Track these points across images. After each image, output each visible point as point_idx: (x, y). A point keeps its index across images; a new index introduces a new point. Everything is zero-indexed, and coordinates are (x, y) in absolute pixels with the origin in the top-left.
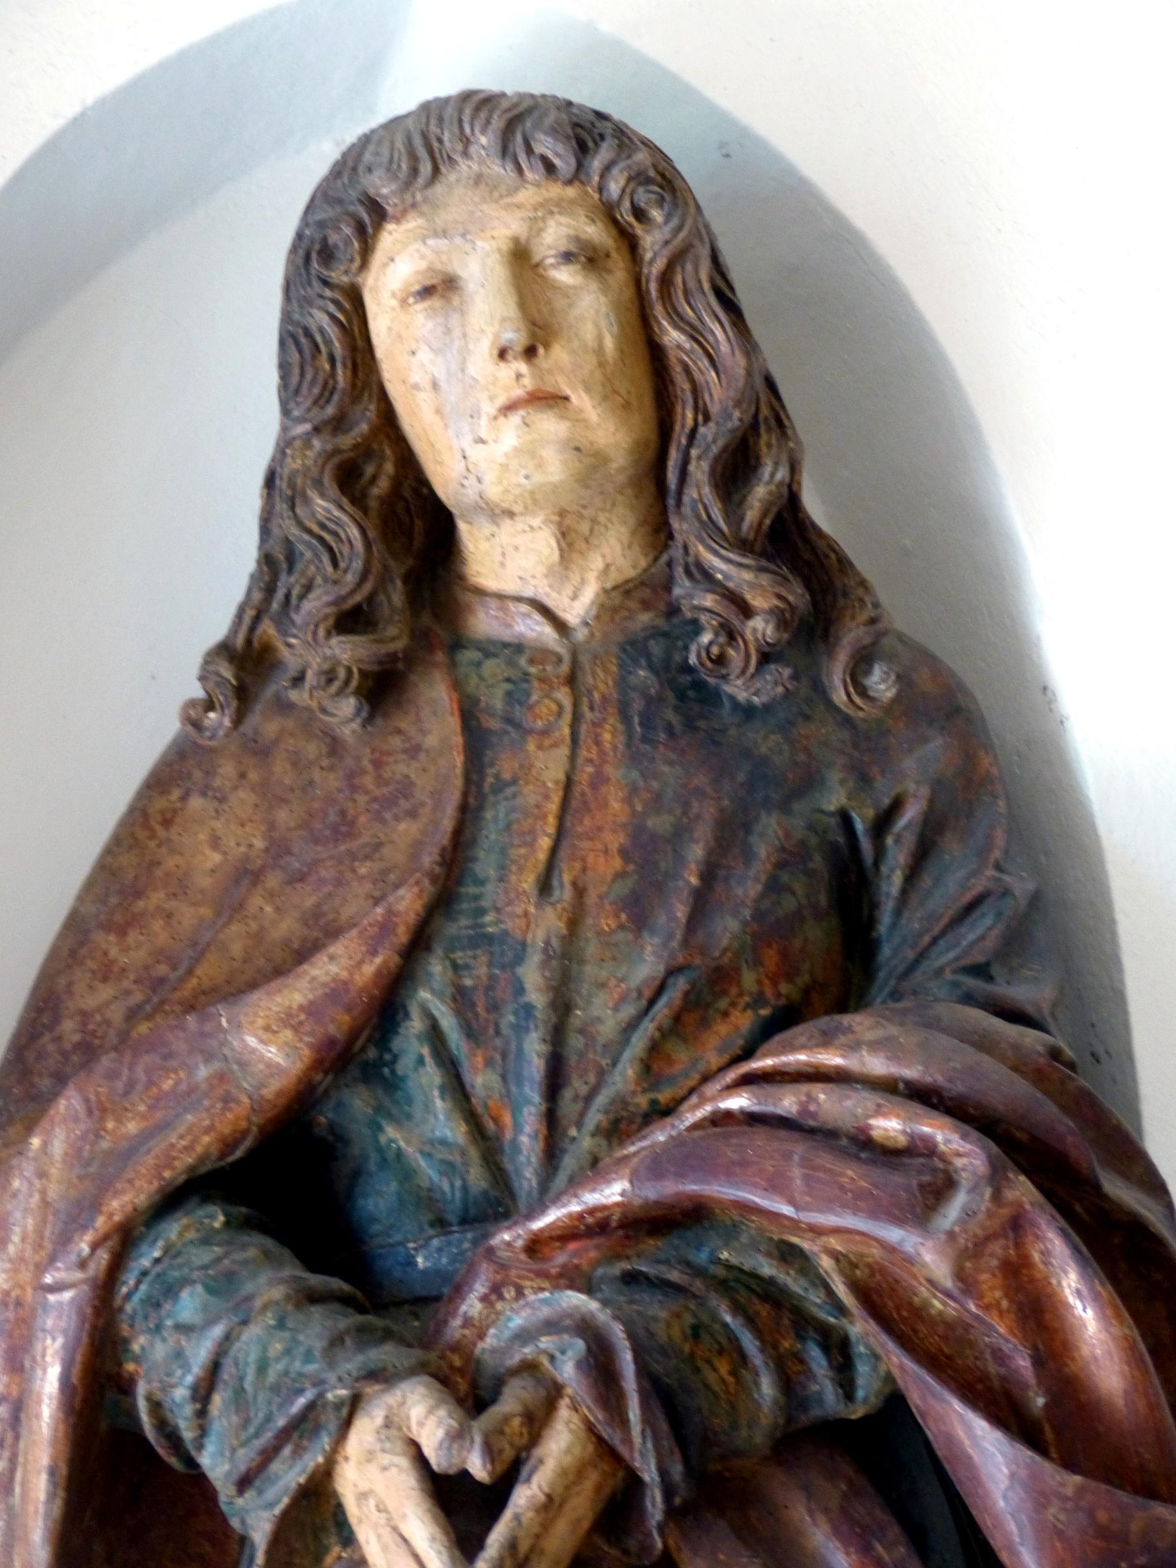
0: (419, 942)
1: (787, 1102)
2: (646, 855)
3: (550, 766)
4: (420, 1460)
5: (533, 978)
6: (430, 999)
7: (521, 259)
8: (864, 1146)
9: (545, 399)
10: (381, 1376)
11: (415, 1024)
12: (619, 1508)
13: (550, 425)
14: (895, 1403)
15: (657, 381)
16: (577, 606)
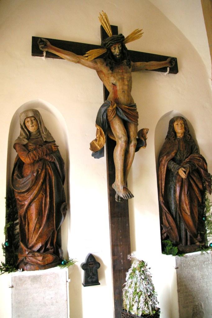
0: (178, 150)
1: (194, 157)
2: (185, 146)
3: (181, 143)
4: (183, 171)
5: (182, 152)
6: (178, 153)
7: (181, 123)
8: (197, 159)
9: (182, 129)
10: (181, 167)
11: (178, 154)
12: (189, 172)
13: (182, 130)
14: (198, 169)
15: (185, 128)
16: (181, 137)
